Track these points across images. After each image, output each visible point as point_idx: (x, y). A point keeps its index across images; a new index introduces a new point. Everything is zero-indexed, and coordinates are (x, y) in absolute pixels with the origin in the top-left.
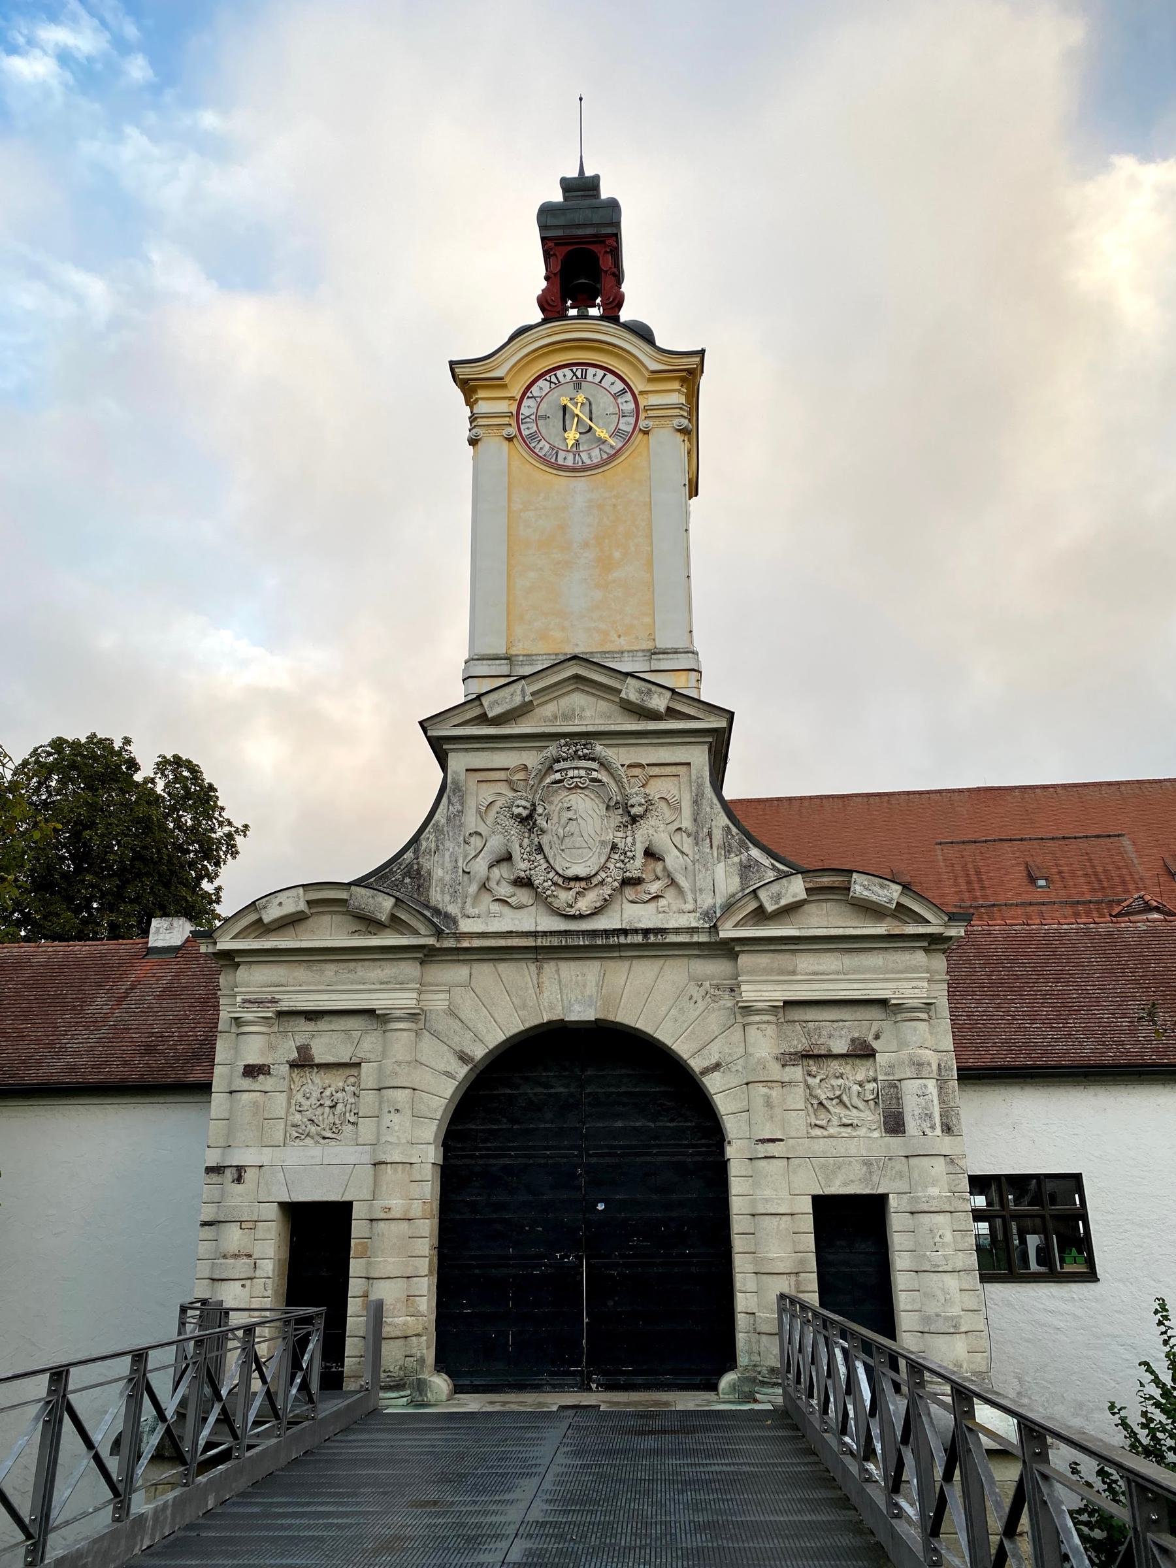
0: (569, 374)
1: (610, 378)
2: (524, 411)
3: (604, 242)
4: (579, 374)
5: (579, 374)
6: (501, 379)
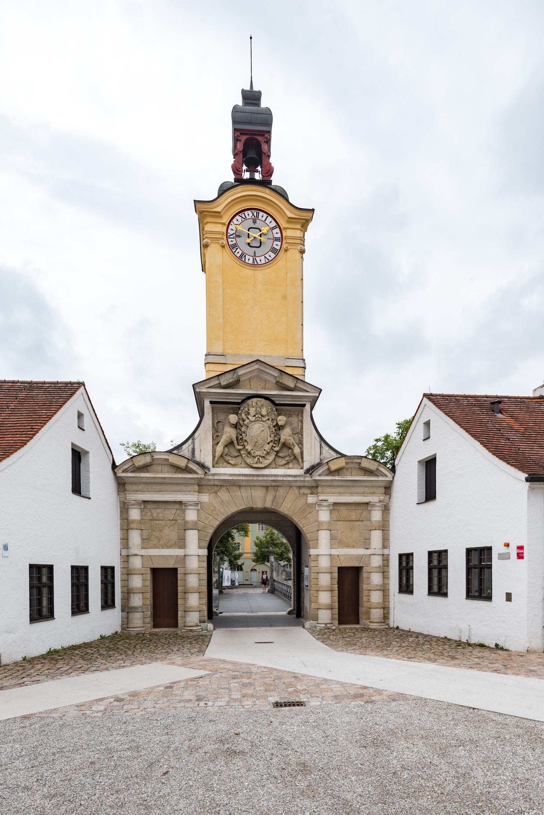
0: (251, 214)
1: (269, 219)
2: (229, 231)
3: (264, 135)
4: (255, 214)
5: (255, 214)
6: (219, 212)
